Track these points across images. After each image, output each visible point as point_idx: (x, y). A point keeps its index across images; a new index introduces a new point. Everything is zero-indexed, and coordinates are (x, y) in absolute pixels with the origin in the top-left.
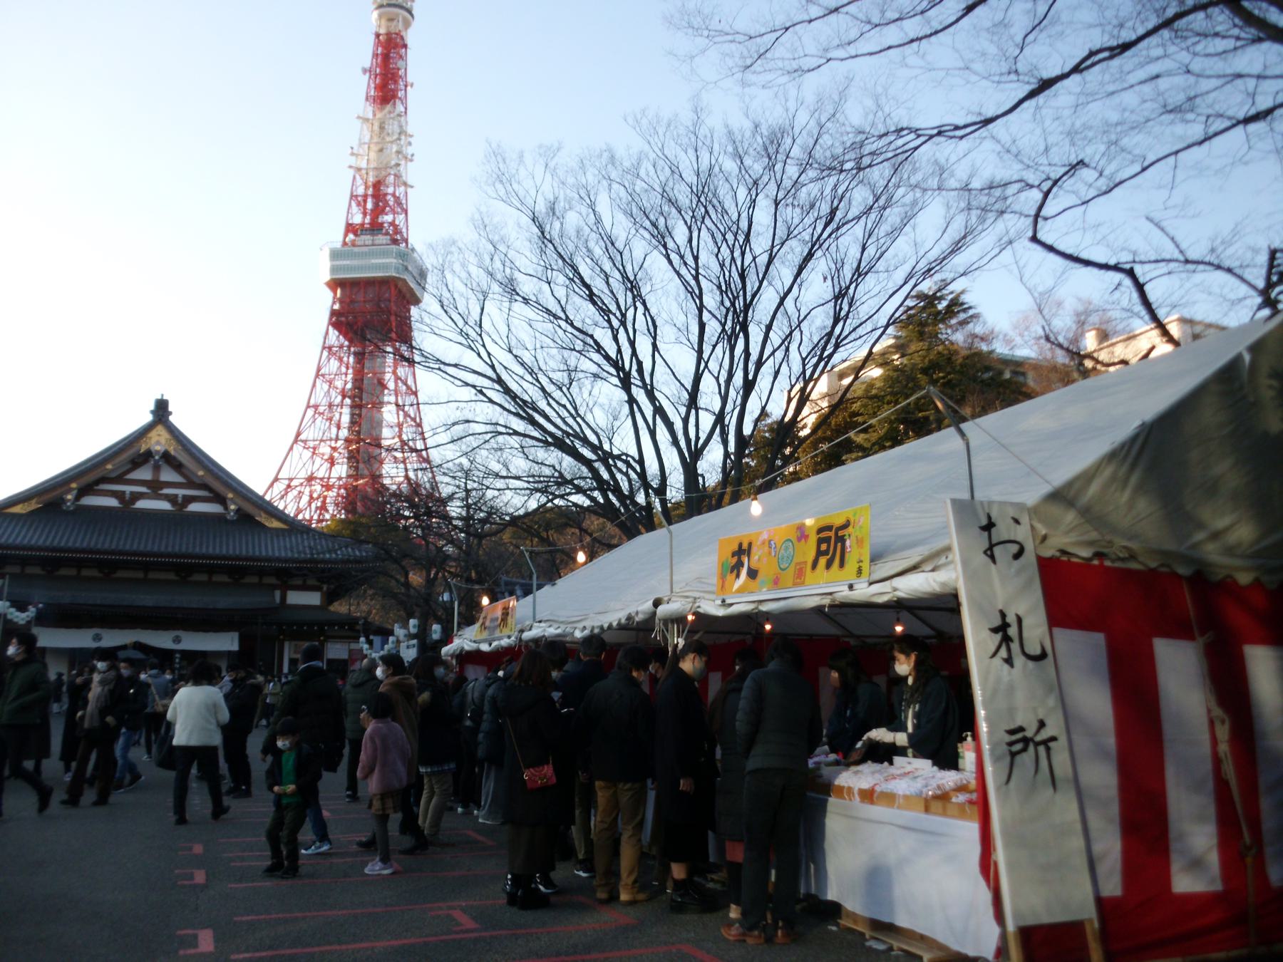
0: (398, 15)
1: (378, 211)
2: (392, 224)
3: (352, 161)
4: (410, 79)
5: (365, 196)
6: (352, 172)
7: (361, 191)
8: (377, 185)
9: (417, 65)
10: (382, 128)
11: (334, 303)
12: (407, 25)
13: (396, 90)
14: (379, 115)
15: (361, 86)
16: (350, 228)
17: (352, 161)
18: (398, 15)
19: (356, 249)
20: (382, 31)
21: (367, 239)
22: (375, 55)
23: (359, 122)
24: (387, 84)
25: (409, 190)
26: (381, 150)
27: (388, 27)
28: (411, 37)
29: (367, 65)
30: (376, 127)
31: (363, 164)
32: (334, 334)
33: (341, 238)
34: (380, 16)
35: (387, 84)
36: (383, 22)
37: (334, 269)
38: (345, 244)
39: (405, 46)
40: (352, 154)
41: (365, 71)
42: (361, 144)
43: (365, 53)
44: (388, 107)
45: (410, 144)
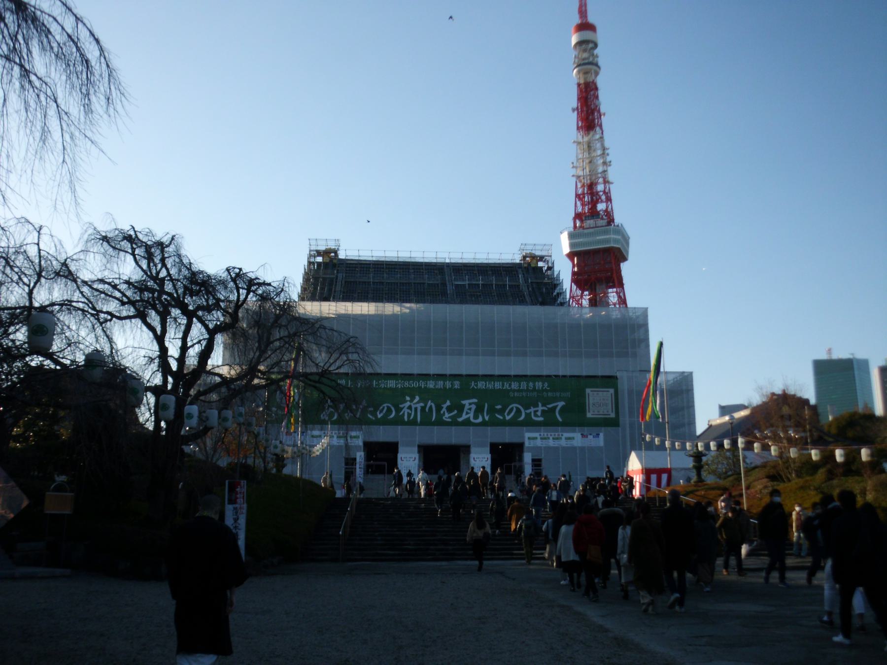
0: (591, 70)
1: (594, 203)
2: (606, 211)
3: (574, 172)
4: (602, 111)
5: (583, 194)
6: (574, 179)
7: (580, 192)
8: (591, 186)
9: (606, 100)
10: (589, 147)
11: (573, 267)
12: (597, 74)
13: (594, 120)
14: (586, 139)
15: (572, 119)
16: (578, 216)
17: (574, 172)
18: (591, 70)
19: (586, 231)
20: (582, 82)
21: (590, 223)
22: (579, 99)
24: (589, 115)
25: (611, 186)
26: (590, 162)
27: (585, 79)
28: (601, 81)
29: (575, 106)
30: (586, 146)
31: (581, 173)
32: (574, 287)
33: (572, 225)
34: (579, 72)
35: (589, 115)
36: (581, 75)
37: (572, 245)
39: (596, 89)
41: (573, 110)
42: (578, 160)
43: (572, 99)
44: (592, 133)
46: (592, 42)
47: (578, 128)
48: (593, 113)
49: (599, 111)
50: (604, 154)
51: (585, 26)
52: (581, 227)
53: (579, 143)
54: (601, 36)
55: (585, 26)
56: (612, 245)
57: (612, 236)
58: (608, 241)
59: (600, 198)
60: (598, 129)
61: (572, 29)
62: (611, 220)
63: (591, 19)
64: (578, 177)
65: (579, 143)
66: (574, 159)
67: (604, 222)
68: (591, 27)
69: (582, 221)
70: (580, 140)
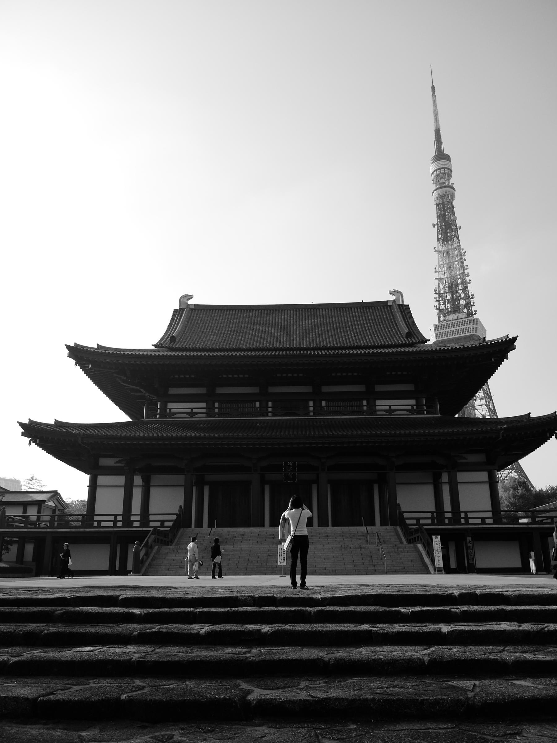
3: (436, 275)
4: (458, 225)
6: (437, 281)
17: (436, 275)
21: (453, 316)
23: (436, 254)
24: (447, 228)
26: (450, 267)
29: (435, 222)
31: (442, 277)
35: (447, 228)
38: (439, 321)
39: (453, 207)
40: (436, 272)
41: (434, 226)
45: (465, 260)
46: (448, 169)
47: (438, 240)
48: (450, 227)
49: (456, 225)
50: (462, 261)
51: (441, 156)
52: (444, 320)
53: (440, 252)
54: (455, 164)
55: (441, 156)
56: (472, 333)
57: (471, 326)
58: (468, 330)
59: (460, 296)
60: (455, 239)
61: (430, 162)
62: (470, 314)
63: (446, 151)
64: (440, 279)
65: (440, 252)
66: (436, 264)
67: (465, 315)
68: (447, 158)
69: (445, 316)
70: (441, 249)
